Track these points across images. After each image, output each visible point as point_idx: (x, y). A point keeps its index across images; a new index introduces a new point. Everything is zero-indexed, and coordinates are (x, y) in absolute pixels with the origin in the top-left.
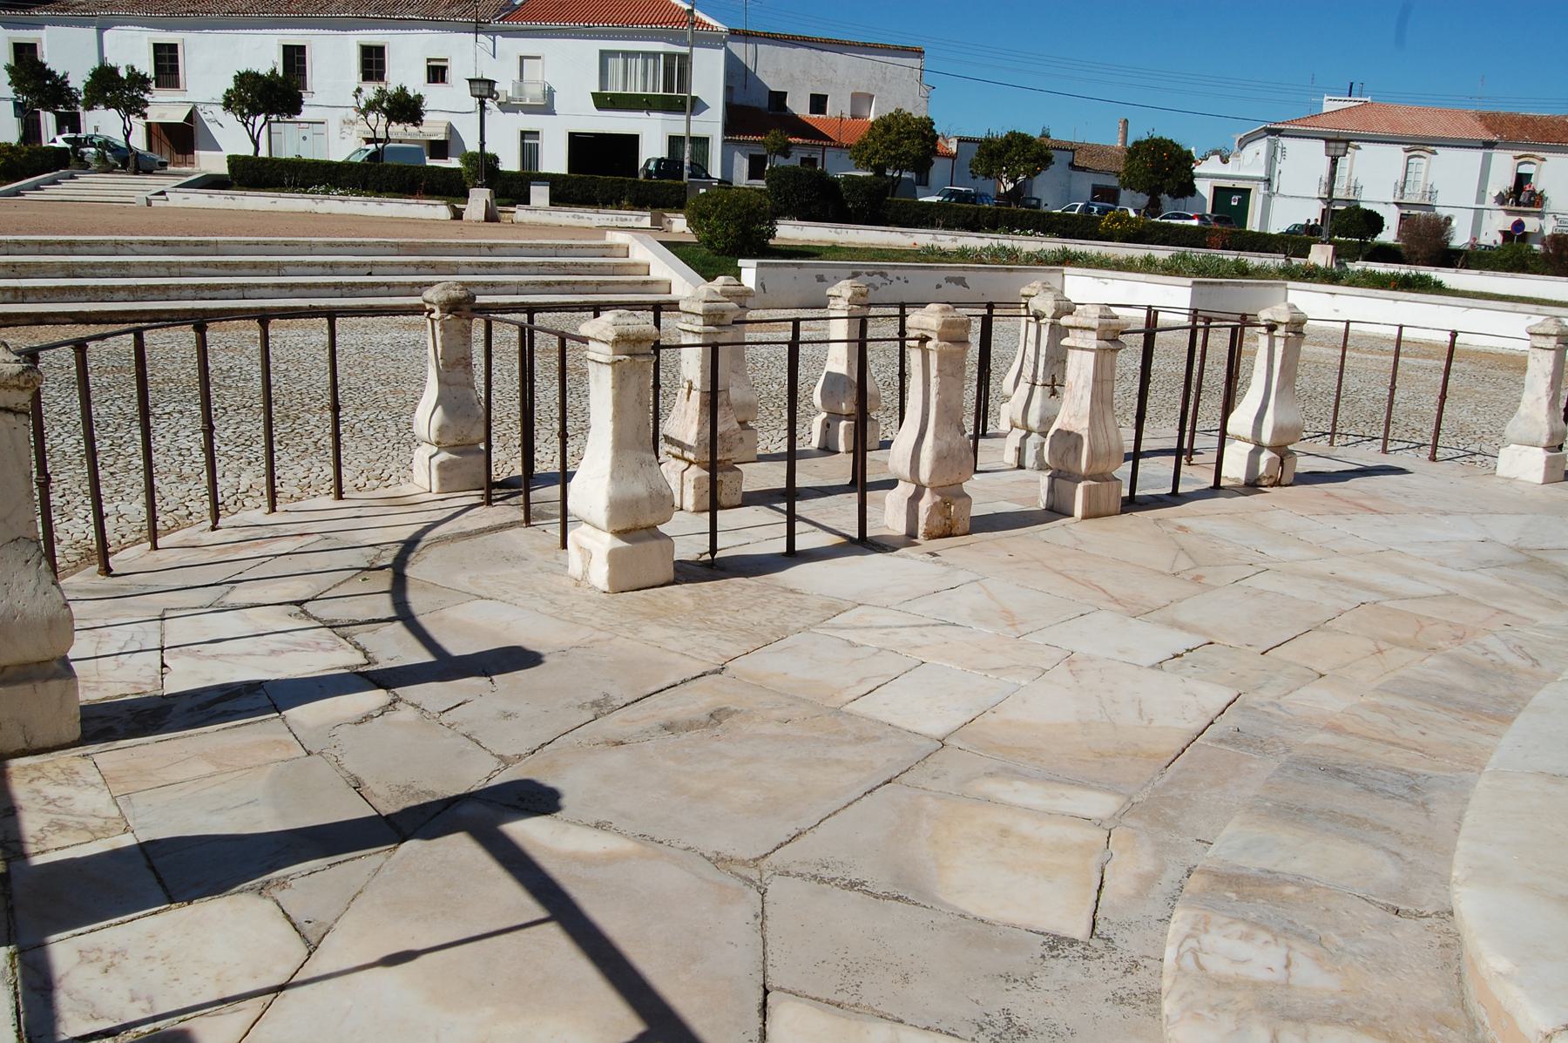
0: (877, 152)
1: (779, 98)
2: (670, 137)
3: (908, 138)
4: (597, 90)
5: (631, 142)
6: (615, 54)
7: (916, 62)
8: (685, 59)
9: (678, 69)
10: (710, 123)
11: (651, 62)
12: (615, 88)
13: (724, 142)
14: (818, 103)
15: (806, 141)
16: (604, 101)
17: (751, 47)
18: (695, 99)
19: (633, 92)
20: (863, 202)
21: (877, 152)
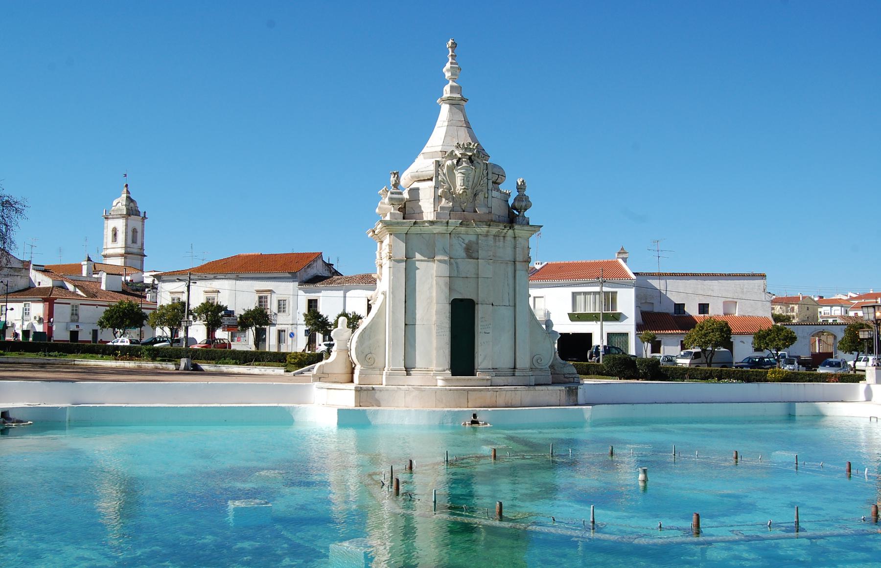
0: (695, 340)
1: (680, 307)
2: (608, 334)
3: (713, 332)
4: (571, 312)
5: (588, 337)
6: (579, 293)
7: (759, 282)
8: (614, 294)
9: (610, 299)
10: (628, 326)
11: (597, 296)
12: (580, 310)
13: (636, 334)
14: (704, 308)
15: (684, 332)
16: (575, 317)
17: (663, 282)
18: (620, 314)
19: (589, 312)
20: (646, 370)
21: (695, 340)
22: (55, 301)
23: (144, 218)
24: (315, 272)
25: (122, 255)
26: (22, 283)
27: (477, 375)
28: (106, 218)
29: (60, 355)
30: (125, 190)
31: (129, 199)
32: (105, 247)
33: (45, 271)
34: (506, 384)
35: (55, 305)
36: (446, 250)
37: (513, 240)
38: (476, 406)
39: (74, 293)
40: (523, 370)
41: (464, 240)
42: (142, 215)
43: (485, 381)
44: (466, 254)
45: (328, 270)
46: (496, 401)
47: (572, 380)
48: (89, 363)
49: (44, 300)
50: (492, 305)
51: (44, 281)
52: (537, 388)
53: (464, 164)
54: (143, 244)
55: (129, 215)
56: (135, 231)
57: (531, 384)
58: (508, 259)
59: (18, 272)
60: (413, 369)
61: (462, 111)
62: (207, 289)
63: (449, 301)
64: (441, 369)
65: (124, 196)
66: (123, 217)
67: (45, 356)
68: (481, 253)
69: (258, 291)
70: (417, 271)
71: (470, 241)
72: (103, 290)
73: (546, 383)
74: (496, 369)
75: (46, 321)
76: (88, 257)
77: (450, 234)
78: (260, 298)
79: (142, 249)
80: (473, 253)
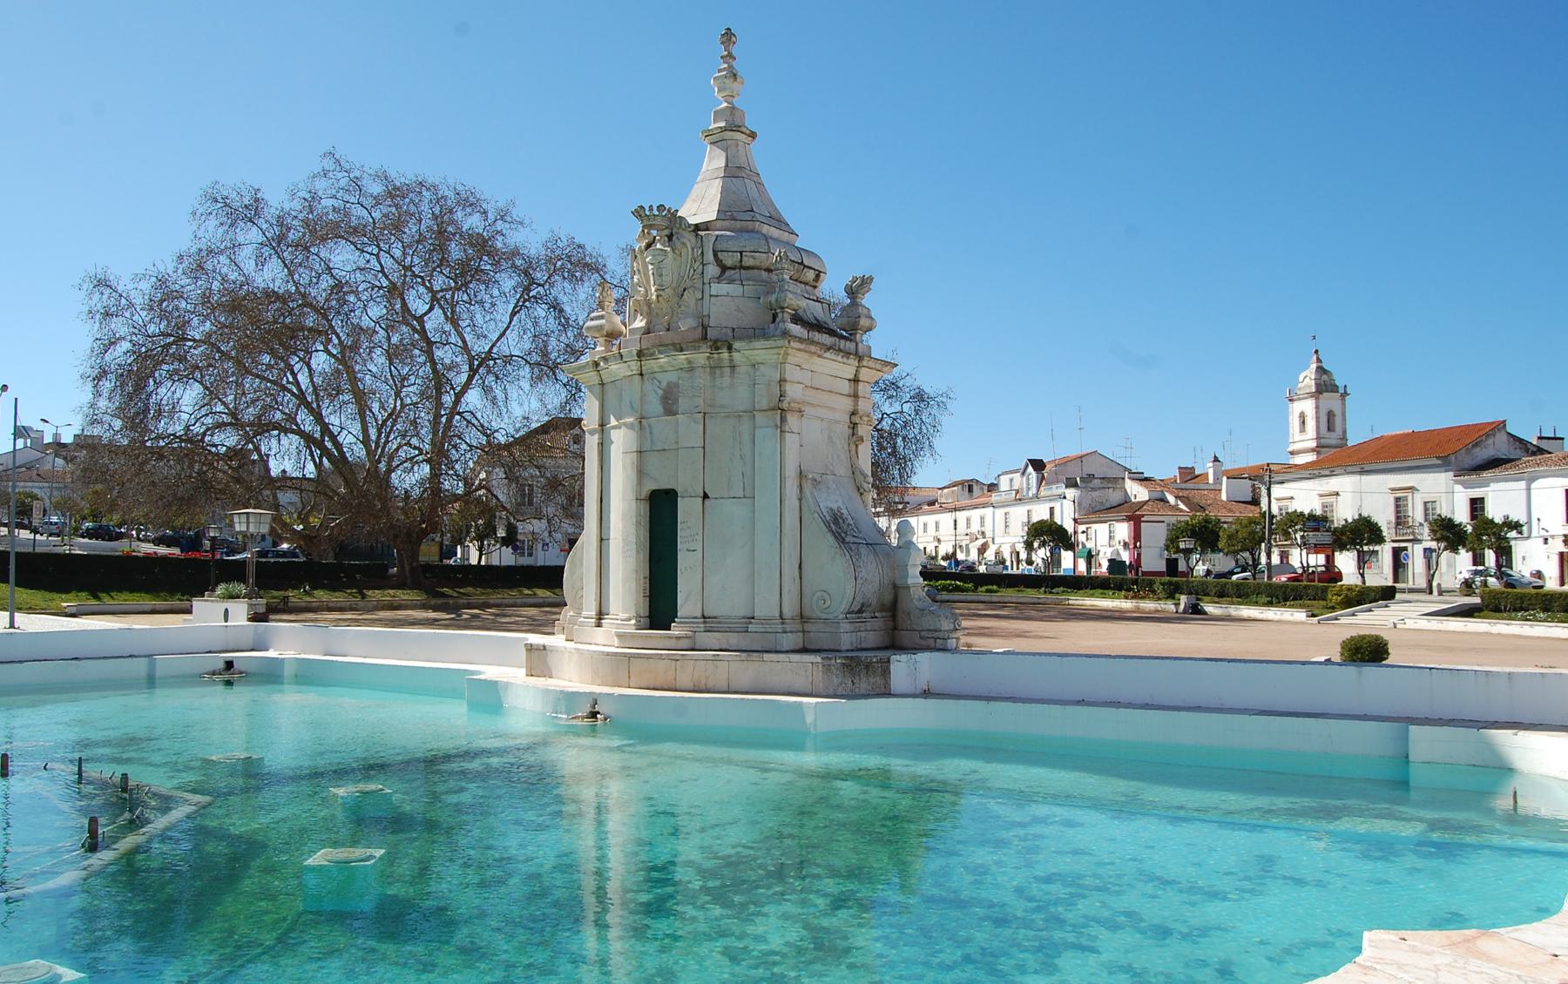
22: (1142, 519)
23: (1345, 394)
24: (1492, 453)
25: (1313, 450)
26: (1114, 497)
27: (672, 628)
28: (1290, 400)
29: (1064, 592)
30: (1315, 358)
31: (1321, 370)
32: (1291, 441)
33: (1145, 481)
34: (724, 647)
35: (1142, 524)
36: (634, 405)
37: (750, 370)
38: (658, 684)
39: (1176, 508)
40: (767, 620)
41: (660, 382)
42: (1341, 390)
43: (674, 640)
44: (664, 408)
45: (1521, 448)
46: (675, 679)
47: (931, 642)
48: (1085, 602)
49: (1129, 519)
50: (705, 496)
51: (1138, 493)
52: (767, 656)
53: (659, 246)
54: (1344, 432)
55: (1321, 393)
56: (1330, 415)
57: (778, 649)
58: (741, 408)
59: (1112, 483)
60: (606, 617)
61: (726, 150)
62: (1321, 492)
63: (639, 491)
64: (626, 616)
65: (1314, 366)
66: (1312, 397)
67: (1045, 592)
68: (683, 403)
69: (1393, 490)
70: (613, 447)
71: (671, 382)
72: (1222, 501)
73: (832, 647)
74: (715, 618)
75: (1131, 547)
76: (1215, 456)
77: (641, 375)
78: (1397, 500)
79: (1344, 438)
80: (673, 403)
